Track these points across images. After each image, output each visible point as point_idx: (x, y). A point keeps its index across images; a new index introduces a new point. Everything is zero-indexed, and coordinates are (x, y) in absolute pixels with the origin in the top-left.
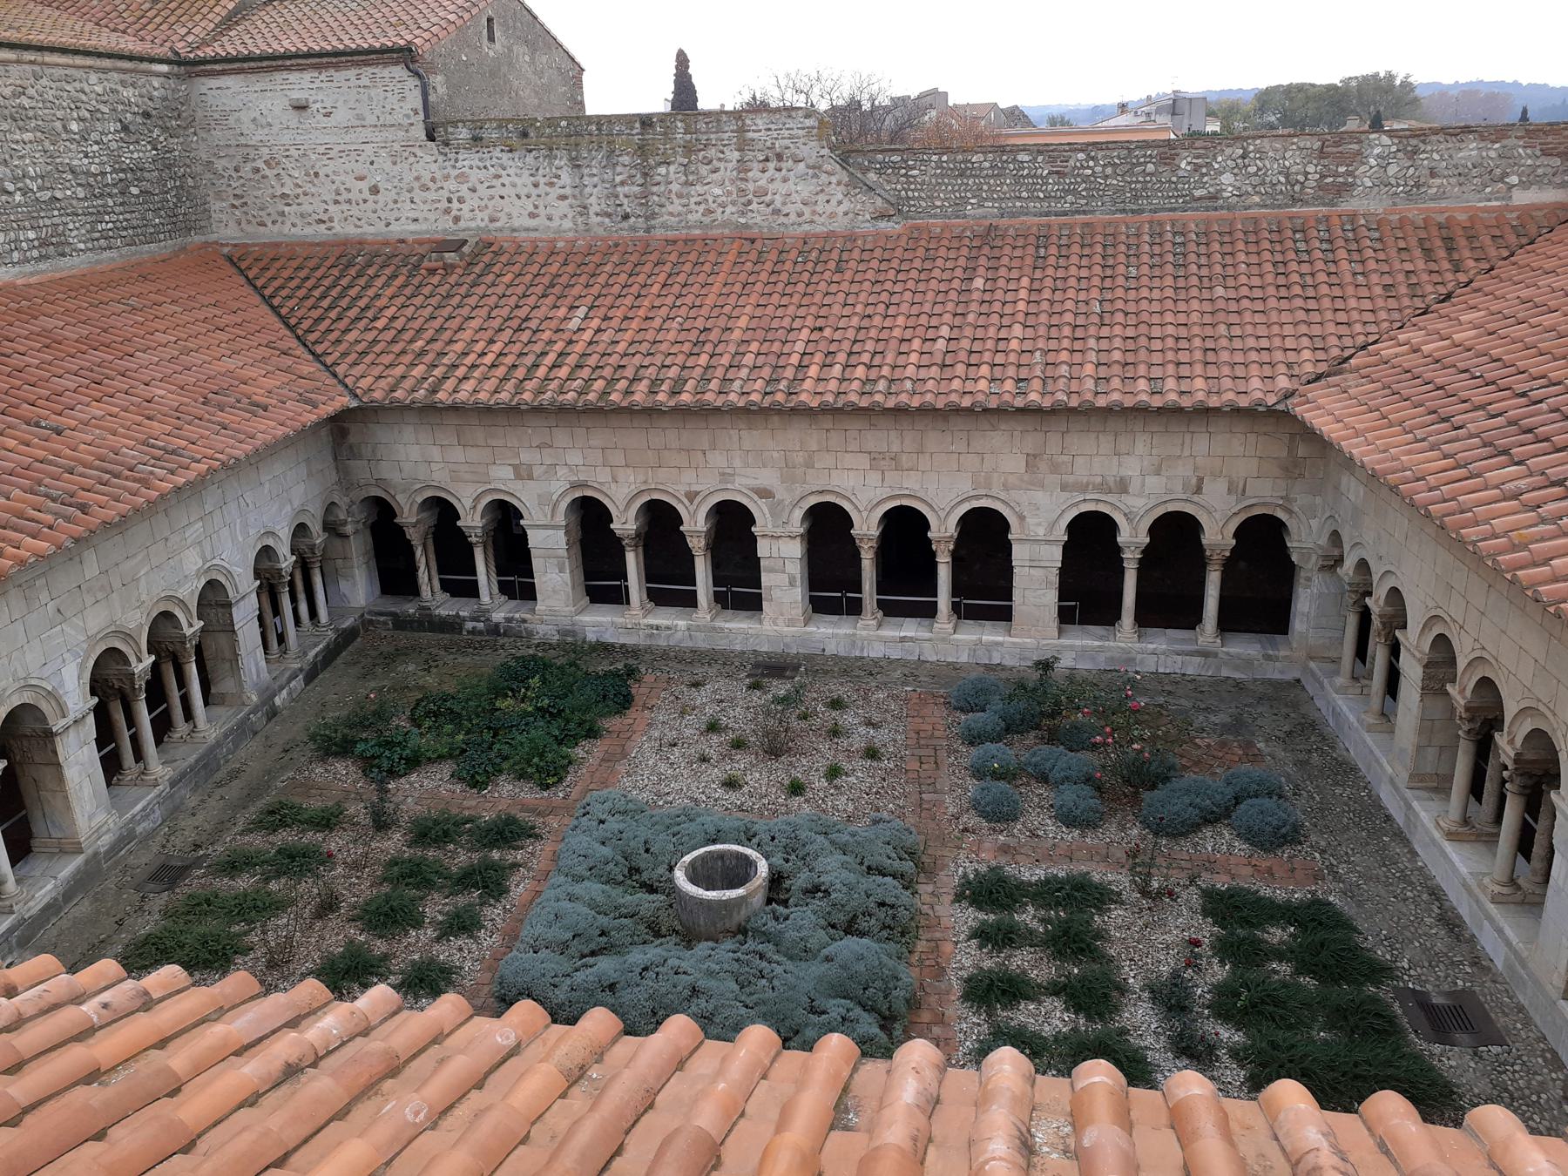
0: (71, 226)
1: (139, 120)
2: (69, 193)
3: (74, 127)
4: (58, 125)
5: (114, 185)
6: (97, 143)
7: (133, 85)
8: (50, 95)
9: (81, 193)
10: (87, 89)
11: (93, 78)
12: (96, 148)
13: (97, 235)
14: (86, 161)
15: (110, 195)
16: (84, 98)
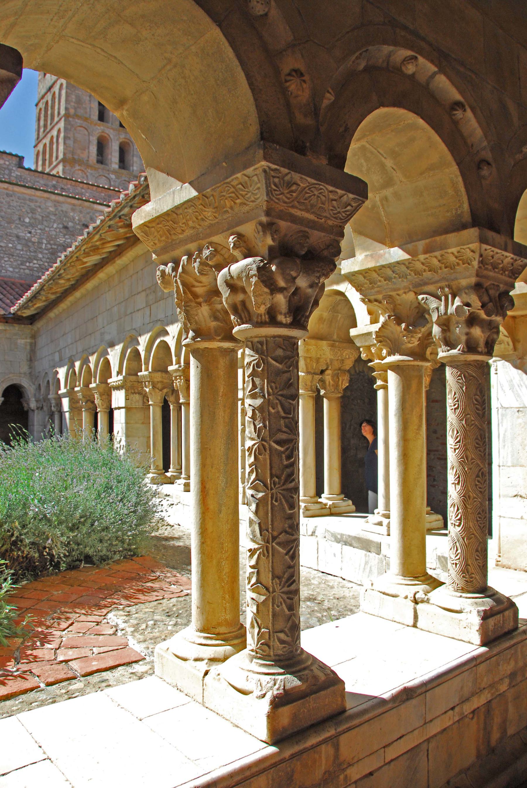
0: (6, 259)
1: (79, 227)
2: (10, 245)
3: (27, 220)
4: (16, 217)
5: (47, 250)
6: (40, 229)
7: (81, 212)
8: (15, 204)
9: (19, 247)
10: (43, 206)
11: (49, 204)
12: (39, 231)
13: (23, 267)
14: (29, 235)
15: (41, 253)
16: (39, 210)
